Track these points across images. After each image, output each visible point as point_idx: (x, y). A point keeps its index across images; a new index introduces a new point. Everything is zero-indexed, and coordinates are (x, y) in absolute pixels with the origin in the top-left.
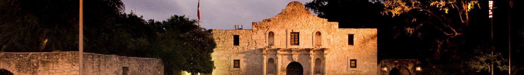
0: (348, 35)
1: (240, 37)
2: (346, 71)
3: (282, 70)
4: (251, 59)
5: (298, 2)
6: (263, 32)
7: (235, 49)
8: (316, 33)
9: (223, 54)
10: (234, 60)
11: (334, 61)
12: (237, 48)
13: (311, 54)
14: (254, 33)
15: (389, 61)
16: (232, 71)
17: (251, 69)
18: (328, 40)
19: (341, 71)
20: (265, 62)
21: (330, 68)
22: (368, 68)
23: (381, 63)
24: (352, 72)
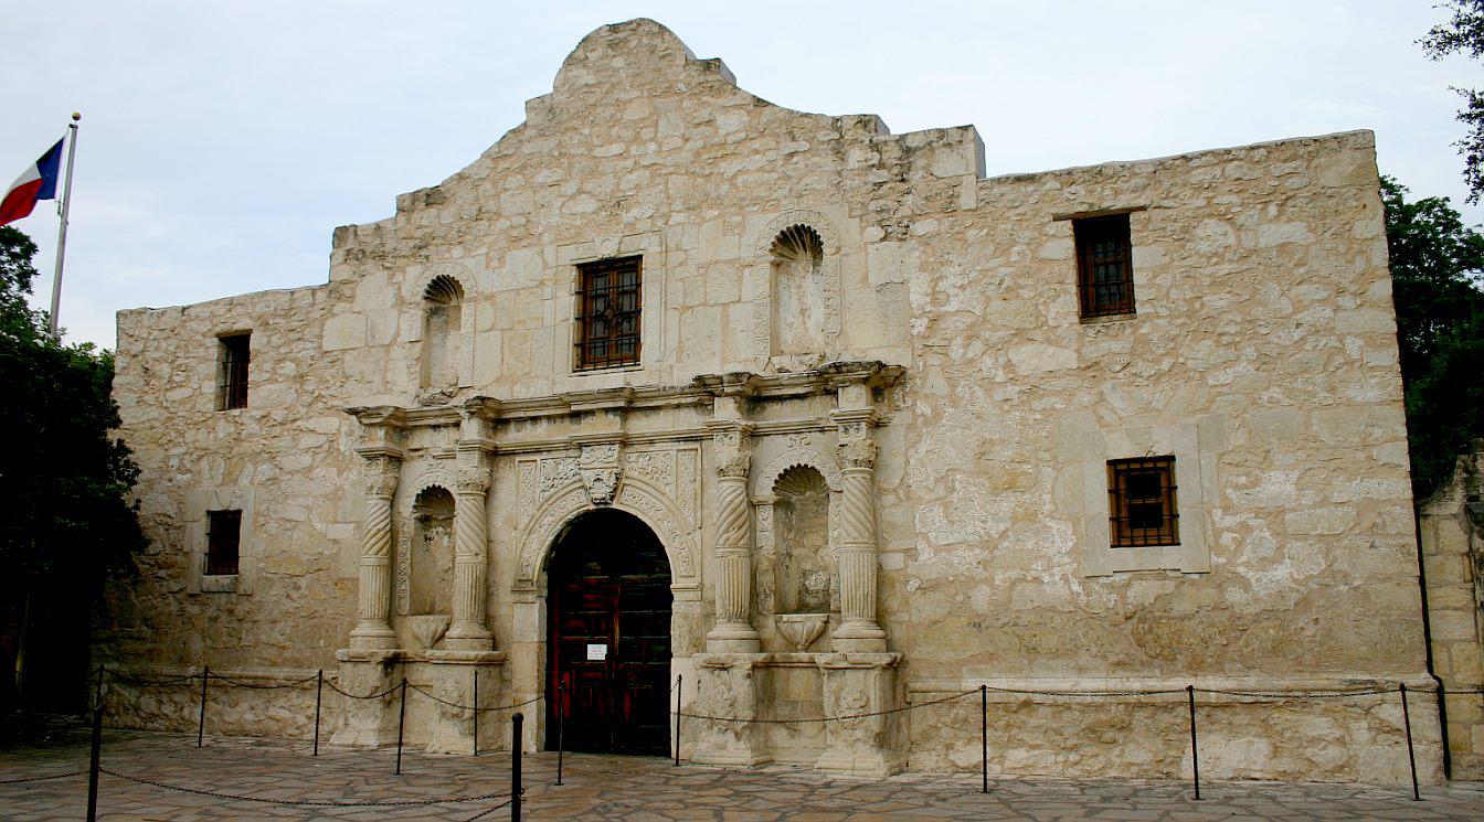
0: (1069, 224)
2: (1064, 578)
3: (521, 586)
4: (310, 501)
5: (641, 22)
6: (391, 291)
7: (220, 436)
9: (155, 475)
10: (209, 513)
11: (940, 491)
12: (232, 429)
13: (726, 429)
17: (303, 582)
18: (881, 288)
19: (1024, 579)
21: (911, 553)
22: (1305, 536)
23: (1459, 475)
24: (1128, 584)
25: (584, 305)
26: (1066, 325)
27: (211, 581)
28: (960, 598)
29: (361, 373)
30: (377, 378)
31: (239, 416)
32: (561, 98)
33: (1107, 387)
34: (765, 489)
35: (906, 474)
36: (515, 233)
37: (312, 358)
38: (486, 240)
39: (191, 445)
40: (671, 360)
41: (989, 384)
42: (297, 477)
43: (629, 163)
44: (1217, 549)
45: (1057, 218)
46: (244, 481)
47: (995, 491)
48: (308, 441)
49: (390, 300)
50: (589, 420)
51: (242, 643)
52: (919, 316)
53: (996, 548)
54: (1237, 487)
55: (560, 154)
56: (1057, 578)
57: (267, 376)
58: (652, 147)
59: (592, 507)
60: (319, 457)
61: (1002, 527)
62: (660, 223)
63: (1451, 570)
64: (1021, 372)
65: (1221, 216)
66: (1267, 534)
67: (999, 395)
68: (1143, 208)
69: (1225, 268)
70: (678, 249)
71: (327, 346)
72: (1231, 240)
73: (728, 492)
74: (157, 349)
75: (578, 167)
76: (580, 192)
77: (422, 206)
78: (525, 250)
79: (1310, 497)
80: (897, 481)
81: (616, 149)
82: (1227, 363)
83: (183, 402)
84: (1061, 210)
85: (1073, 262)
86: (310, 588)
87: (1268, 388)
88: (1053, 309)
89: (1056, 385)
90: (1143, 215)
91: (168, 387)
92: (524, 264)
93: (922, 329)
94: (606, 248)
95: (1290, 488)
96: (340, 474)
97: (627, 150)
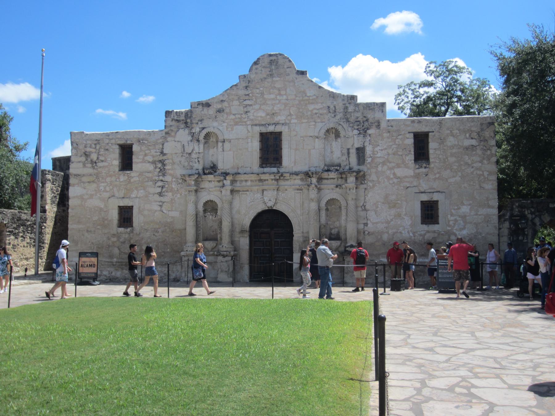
0: (412, 134)
2: (408, 232)
3: (242, 232)
4: (161, 204)
8: (328, 131)
9: (93, 193)
10: (119, 207)
12: (127, 177)
14: (169, 139)
15: (532, 202)
16: (114, 235)
17: (160, 231)
18: (358, 149)
19: (397, 232)
20: (191, 209)
21: (366, 224)
22: (471, 223)
24: (425, 234)
25: (262, 145)
26: (410, 163)
27: (122, 230)
28: (379, 237)
29: (180, 162)
30: (186, 164)
31: (129, 174)
32: (252, 76)
33: (421, 181)
34: (323, 204)
35: (365, 202)
36: (237, 120)
37: (159, 155)
38: (227, 121)
39: (109, 183)
40: (293, 165)
41: (389, 178)
42: (156, 195)
43: (277, 101)
44: (449, 226)
45: (409, 133)
46: (133, 196)
47: (390, 208)
48: (160, 184)
49: (190, 138)
50: (266, 182)
52: (369, 158)
53: (390, 223)
54: (454, 209)
55: (253, 95)
56: (406, 232)
57: (141, 160)
58: (285, 97)
59: (267, 208)
60: (164, 190)
61: (391, 217)
62: (288, 122)
63: (506, 232)
64: (399, 174)
65: (453, 136)
66: (462, 222)
67: (391, 182)
68: (433, 132)
69: (454, 151)
70: (294, 130)
71: (165, 152)
72: (456, 143)
73: (314, 206)
74: (91, 147)
75: (258, 100)
76: (260, 109)
77: (200, 107)
78: (241, 126)
79: (473, 213)
80: (362, 204)
81: (272, 96)
82: (454, 177)
83: (104, 167)
84: (411, 131)
85: (413, 145)
86: (163, 232)
87: (464, 184)
88: (407, 158)
89: (407, 180)
90: (433, 134)
91: (97, 161)
92: (240, 131)
93: (370, 161)
94: (271, 129)
95: (468, 211)
96: (173, 195)
97: (276, 98)
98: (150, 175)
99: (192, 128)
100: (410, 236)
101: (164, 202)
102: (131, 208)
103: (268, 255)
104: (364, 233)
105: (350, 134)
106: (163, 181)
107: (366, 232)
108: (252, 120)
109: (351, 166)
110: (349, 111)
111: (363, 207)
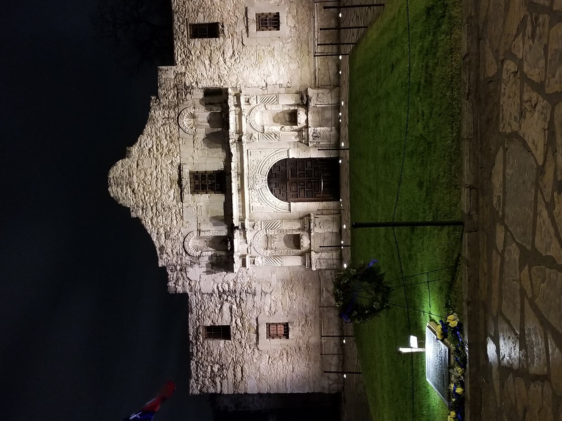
1: (209, 323)
2: (287, 43)
21: (281, 86)
35: (258, 87)
49: (196, 266)
51: (312, 319)
56: (288, 45)
60: (249, 291)
98: (234, 307)
99: (186, 264)
100: (291, 41)
101: (262, 290)
102: (269, 325)
103: (313, 184)
104: (289, 87)
105: (190, 102)
106: (241, 292)
107: (289, 85)
108: (177, 202)
109: (223, 102)
110: (167, 104)
111: (263, 89)
